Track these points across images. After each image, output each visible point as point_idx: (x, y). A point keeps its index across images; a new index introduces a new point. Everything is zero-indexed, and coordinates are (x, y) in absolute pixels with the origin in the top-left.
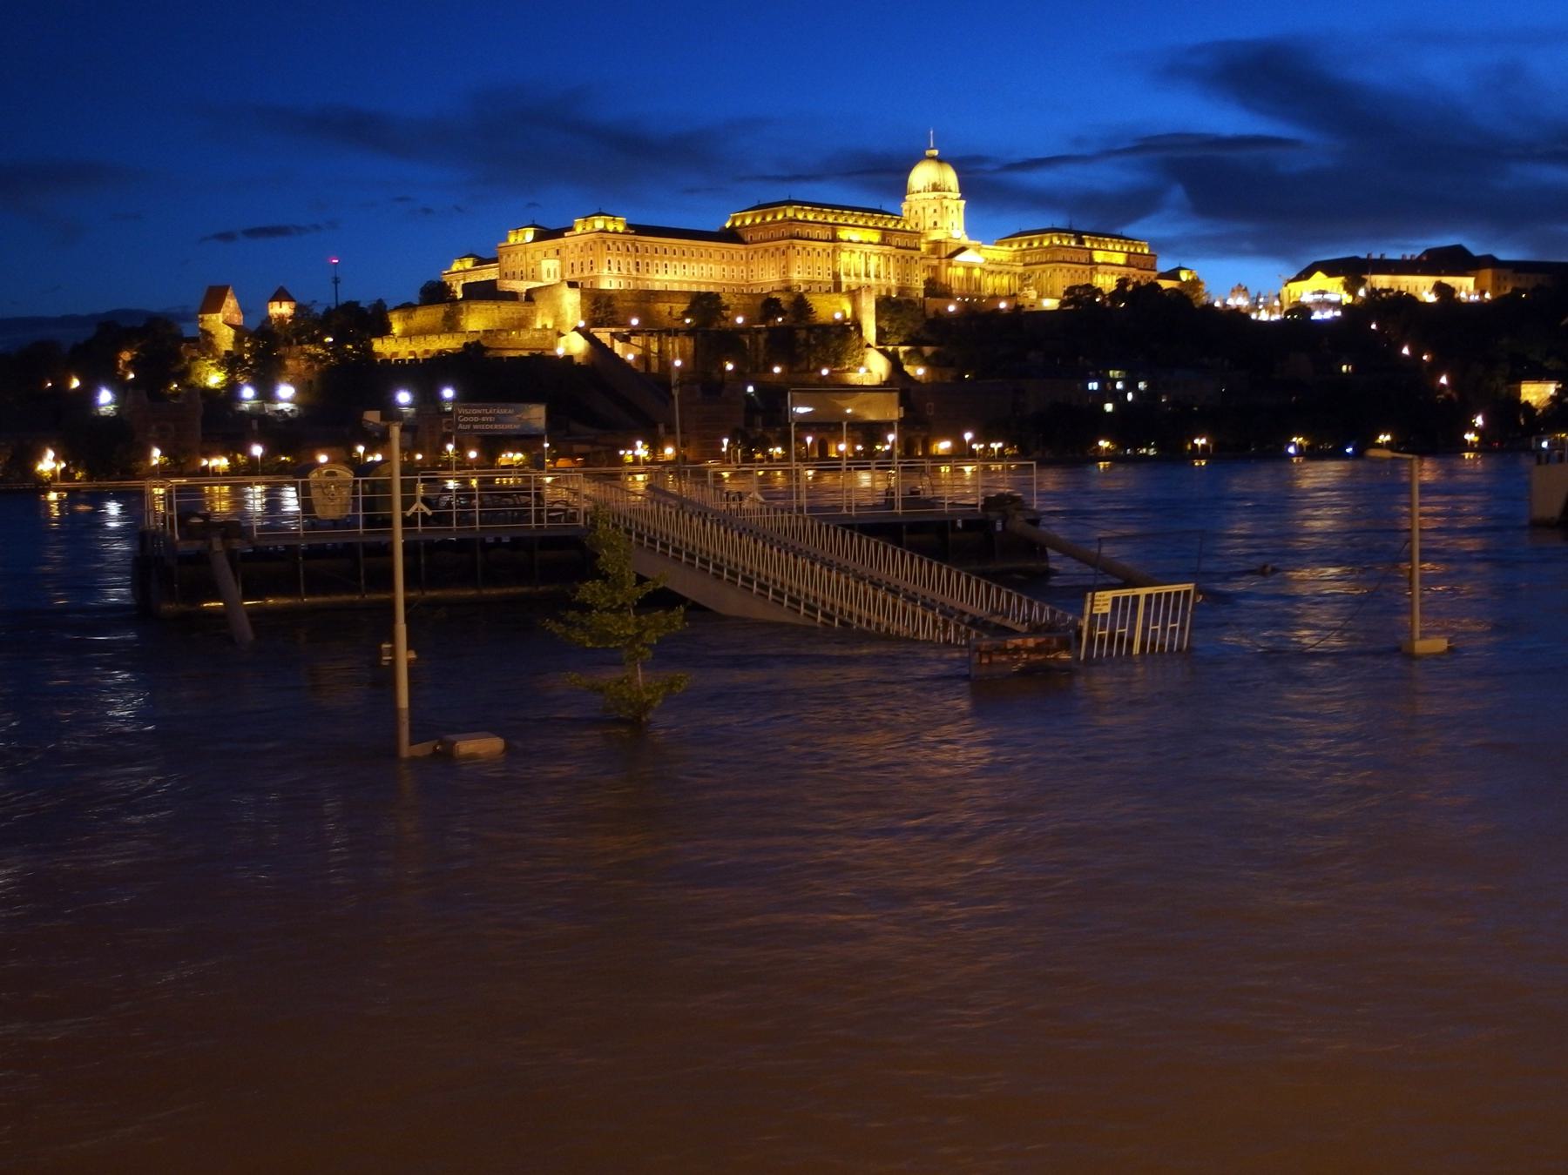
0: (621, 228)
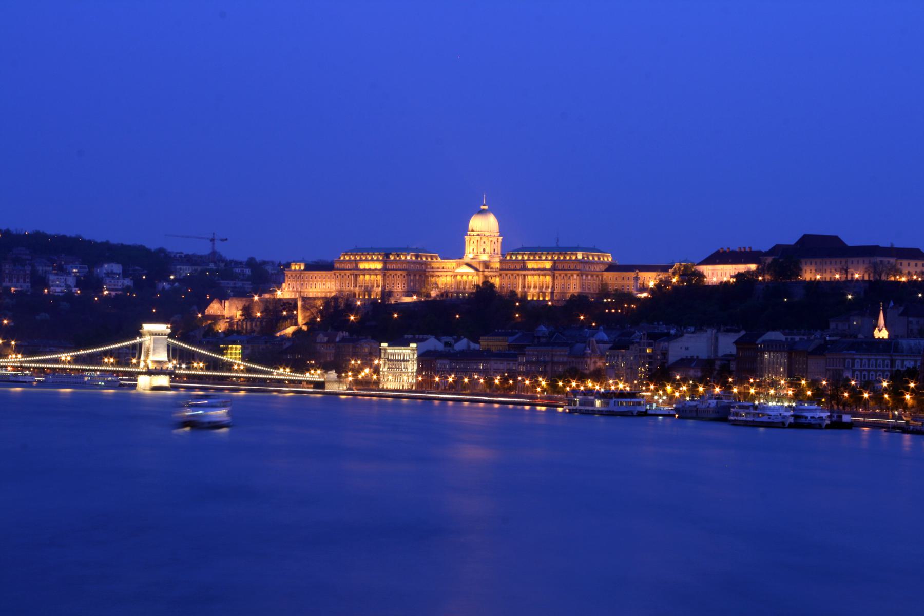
0: (297, 268)
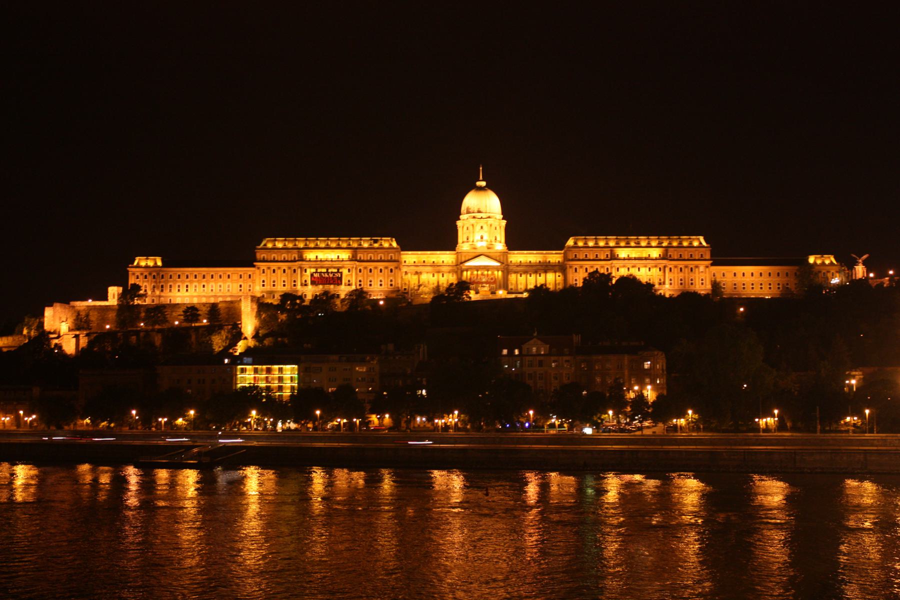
0: (151, 263)
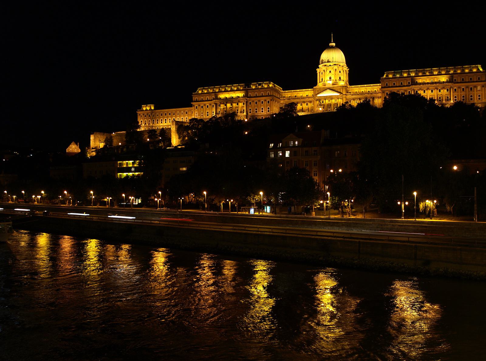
0: (148, 108)
